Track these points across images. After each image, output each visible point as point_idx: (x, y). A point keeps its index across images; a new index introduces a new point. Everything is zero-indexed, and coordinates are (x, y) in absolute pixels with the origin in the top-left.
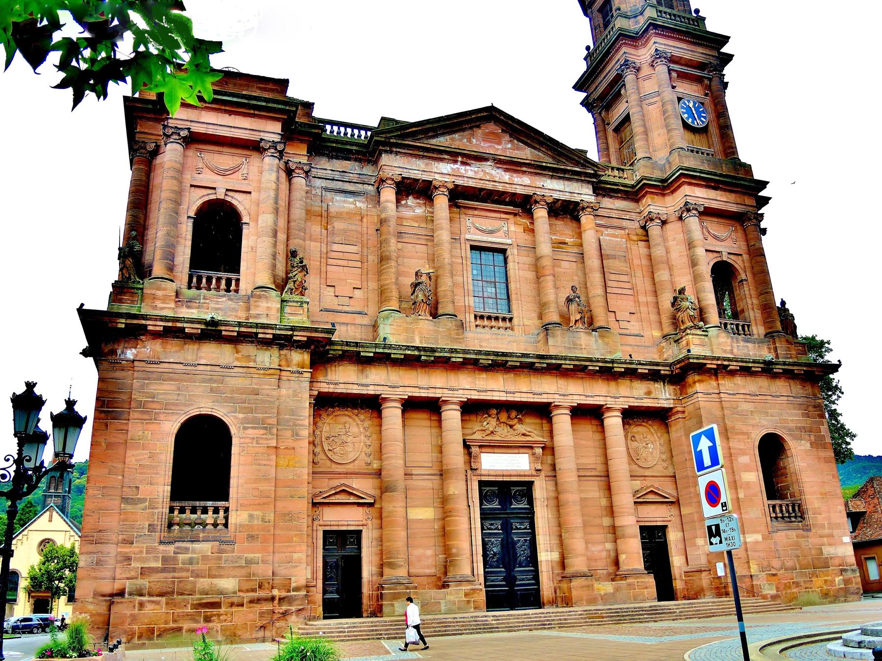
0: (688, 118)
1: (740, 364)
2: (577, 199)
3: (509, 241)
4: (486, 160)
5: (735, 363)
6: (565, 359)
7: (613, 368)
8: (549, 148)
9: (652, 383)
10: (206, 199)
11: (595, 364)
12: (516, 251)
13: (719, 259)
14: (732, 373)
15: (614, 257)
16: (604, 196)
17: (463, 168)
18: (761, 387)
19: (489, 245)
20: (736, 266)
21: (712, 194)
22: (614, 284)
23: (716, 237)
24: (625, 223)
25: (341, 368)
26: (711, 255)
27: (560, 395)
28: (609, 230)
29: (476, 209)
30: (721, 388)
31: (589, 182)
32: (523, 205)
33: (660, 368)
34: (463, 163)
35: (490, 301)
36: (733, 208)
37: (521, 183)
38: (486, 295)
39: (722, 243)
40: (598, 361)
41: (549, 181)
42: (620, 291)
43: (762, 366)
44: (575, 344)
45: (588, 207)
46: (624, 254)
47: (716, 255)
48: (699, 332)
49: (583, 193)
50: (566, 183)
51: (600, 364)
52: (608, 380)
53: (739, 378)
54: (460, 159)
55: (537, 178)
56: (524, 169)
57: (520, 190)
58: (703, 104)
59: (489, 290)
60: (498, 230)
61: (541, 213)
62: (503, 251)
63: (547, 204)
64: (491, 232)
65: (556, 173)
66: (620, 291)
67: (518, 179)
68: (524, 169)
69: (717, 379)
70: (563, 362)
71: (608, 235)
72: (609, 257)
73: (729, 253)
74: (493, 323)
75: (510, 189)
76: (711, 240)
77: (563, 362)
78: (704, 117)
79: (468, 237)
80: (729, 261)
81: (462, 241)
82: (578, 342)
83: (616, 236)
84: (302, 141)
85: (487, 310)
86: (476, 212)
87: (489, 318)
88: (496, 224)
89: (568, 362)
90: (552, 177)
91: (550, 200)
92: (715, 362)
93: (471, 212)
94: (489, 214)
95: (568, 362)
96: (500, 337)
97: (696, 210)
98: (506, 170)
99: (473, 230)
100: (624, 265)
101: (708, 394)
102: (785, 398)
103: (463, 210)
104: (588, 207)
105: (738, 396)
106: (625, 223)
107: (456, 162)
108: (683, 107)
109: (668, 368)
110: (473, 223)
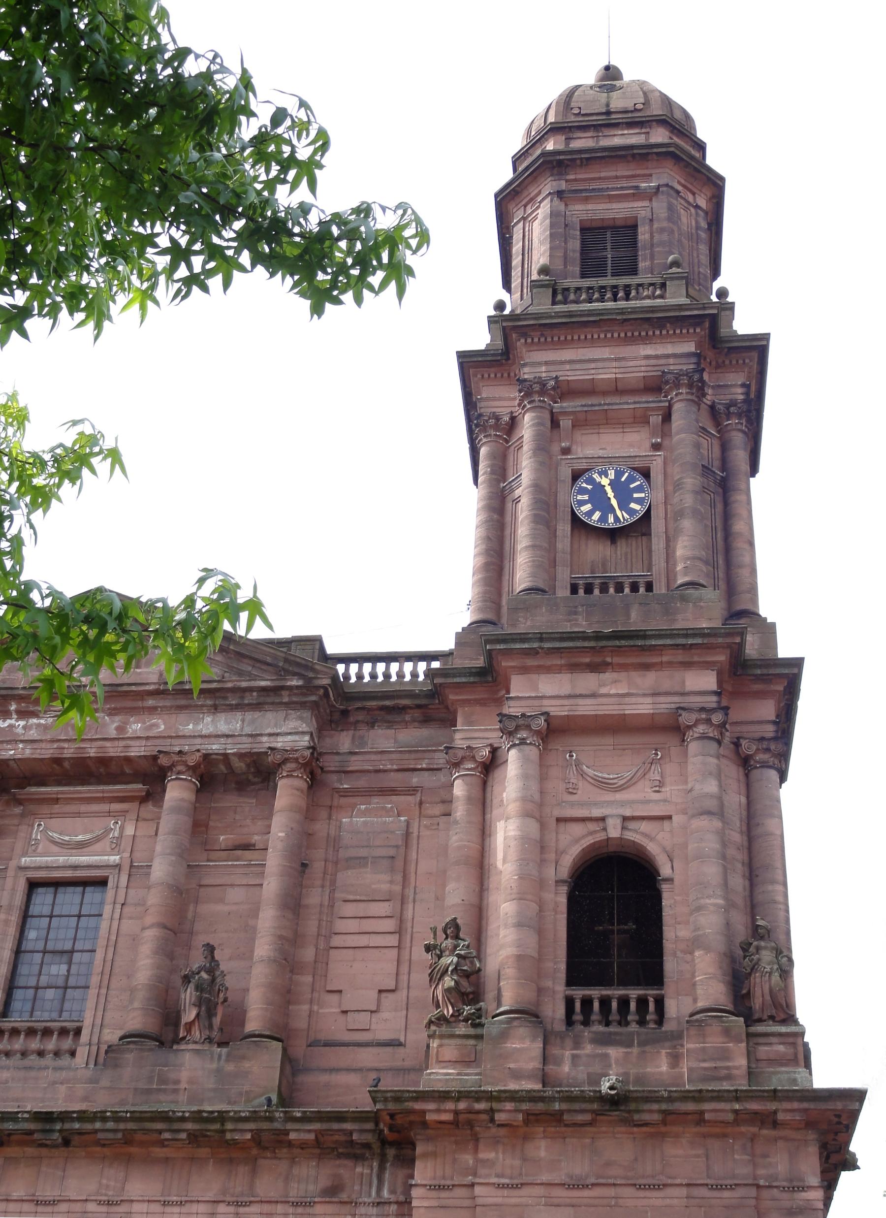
0: (590, 514)
2: (266, 742)
3: (114, 859)
5: (509, 1106)
6: (104, 1119)
7: (287, 1133)
9: (349, 1163)
11: (176, 1126)
12: (124, 879)
14: (518, 1134)
16: (372, 725)
17: (22, 723)
18: (608, 1164)
19: (69, 874)
21: (587, 682)
23: (602, 784)
24: (415, 780)
26: (577, 829)
27: (100, 1203)
28: (375, 800)
29: (56, 801)
30: (482, 1171)
31: (303, 705)
32: (148, 777)
33: (348, 1126)
34: (23, 714)
35: (50, 994)
36: (643, 707)
37: (138, 734)
38: (44, 981)
39: (619, 796)
40: (183, 1119)
41: (208, 719)
42: (363, 940)
44: (163, 1080)
46: (392, 852)
47: (592, 826)
49: (287, 732)
50: (249, 716)
51: (189, 1126)
52: (231, 1161)
54: (13, 707)
55: (183, 716)
56: (151, 702)
57: (137, 750)
58: (646, 474)
59: (54, 970)
60: (98, 839)
61: (177, 792)
62: (102, 883)
63: (190, 768)
65: (217, 698)
66: (363, 940)
67: (135, 727)
69: (476, 1150)
70: (98, 1125)
71: (364, 814)
74: (35, 1044)
75: (113, 750)
77: (98, 1125)
78: (639, 501)
79: (25, 861)
81: (11, 873)
82: (173, 1076)
83: (388, 812)
85: (37, 1014)
87: (31, 1032)
88: (98, 825)
89: (110, 1125)
91: (192, 760)
92: (450, 1105)
93: (45, 809)
94: (84, 808)
95: (110, 1125)
96: (33, 1074)
97: (528, 727)
100: (386, 877)
101: (440, 1188)
103: (32, 807)
104: (285, 761)
105: (525, 1191)
106: (415, 780)
108: (582, 491)
109: (370, 1126)
110: (44, 832)
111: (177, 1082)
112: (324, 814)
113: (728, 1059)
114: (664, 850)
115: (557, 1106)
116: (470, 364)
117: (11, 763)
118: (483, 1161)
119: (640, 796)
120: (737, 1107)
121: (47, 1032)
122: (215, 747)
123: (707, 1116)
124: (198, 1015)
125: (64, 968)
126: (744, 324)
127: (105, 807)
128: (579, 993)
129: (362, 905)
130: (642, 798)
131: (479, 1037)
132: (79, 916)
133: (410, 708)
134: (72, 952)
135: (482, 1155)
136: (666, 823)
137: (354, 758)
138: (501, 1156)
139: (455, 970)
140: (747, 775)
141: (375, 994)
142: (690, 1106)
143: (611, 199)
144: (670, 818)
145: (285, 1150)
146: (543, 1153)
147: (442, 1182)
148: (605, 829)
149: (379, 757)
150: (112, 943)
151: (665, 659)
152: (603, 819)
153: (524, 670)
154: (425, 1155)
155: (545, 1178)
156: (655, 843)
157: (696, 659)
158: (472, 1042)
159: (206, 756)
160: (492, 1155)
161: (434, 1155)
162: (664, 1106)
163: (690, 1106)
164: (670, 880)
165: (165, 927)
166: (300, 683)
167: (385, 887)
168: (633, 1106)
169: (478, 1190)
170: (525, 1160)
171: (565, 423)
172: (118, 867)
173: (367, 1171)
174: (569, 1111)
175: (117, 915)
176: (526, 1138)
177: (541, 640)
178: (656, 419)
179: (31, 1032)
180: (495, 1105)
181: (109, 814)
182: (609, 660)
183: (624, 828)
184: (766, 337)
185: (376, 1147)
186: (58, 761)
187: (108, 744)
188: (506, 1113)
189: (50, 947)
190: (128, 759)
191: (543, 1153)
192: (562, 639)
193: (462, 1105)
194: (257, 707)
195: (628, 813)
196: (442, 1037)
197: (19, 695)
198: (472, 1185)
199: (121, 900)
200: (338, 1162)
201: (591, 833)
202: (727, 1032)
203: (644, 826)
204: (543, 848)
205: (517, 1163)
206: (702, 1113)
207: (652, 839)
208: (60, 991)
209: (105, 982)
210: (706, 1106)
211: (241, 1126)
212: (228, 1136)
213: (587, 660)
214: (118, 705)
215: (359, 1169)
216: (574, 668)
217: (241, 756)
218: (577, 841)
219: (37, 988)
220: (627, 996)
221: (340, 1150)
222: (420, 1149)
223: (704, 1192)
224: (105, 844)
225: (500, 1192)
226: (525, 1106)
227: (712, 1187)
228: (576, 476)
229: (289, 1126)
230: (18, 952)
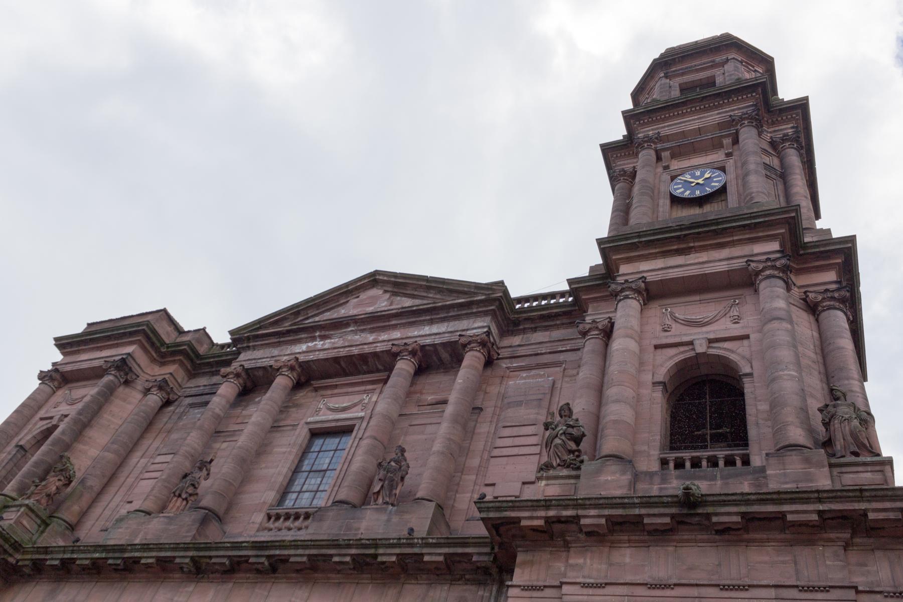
1: (607, 512)
3: (362, 414)
4: (347, 325)
5: (593, 512)
8: (440, 291)
10: (45, 427)
13: (692, 354)
15: (519, 404)
18: (690, 569)
19: (333, 424)
20: (732, 357)
22: (508, 442)
24: (562, 357)
25: (38, 587)
29: (336, 386)
42: (515, 451)
43: (673, 510)
45: (469, 343)
46: (540, 396)
48: (565, 472)
51: (353, 551)
53: (628, 551)
54: (317, 334)
59: (313, 481)
60: (355, 405)
64: (344, 409)
66: (515, 451)
67: (384, 336)
68: (393, 322)
70: (292, 552)
72: (510, 405)
73: (711, 341)
76: (676, 328)
77: (292, 552)
80: (712, 351)
83: (541, 376)
84: (174, 362)
86: (336, 391)
88: (356, 399)
90: (431, 322)
92: (542, 513)
94: (350, 390)
95: (300, 552)
98: (372, 331)
99: (324, 410)
102: (772, 593)
104: (469, 343)
107: (313, 339)
109: (487, 550)
111: (359, 529)
112: (498, 380)
113: (811, 481)
114: (743, 357)
115: (637, 511)
116: (610, 151)
117: (311, 364)
118: (572, 566)
119: (723, 327)
120: (821, 508)
121: (297, 517)
122: (428, 341)
123: (790, 517)
124: (382, 486)
125: (319, 479)
126: (787, 91)
127: (363, 388)
128: (672, 456)
129: (515, 429)
130: (724, 327)
131: (577, 477)
132: (336, 450)
133: (559, 315)
134: (325, 471)
135: (571, 561)
136: (745, 342)
137: (520, 348)
138: (588, 561)
139: (564, 433)
140: (817, 320)
141: (519, 485)
142: (770, 508)
143: (698, 71)
144: (747, 337)
145: (424, 576)
146: (627, 560)
147: (535, 583)
148: (694, 349)
149: (537, 346)
150: (348, 460)
151: (735, 238)
152: (691, 343)
153: (629, 260)
154: (524, 563)
155: (629, 578)
156: (736, 353)
157: (761, 234)
158: (572, 481)
159: (423, 347)
160: (581, 561)
161: (531, 563)
162: (743, 509)
163: (770, 508)
164: (750, 375)
165: (375, 438)
166: (483, 297)
167: (532, 416)
168: (710, 510)
169: (565, 589)
170: (611, 565)
171: (665, 155)
172: (362, 418)
173: (487, 594)
174: (649, 515)
175: (355, 445)
176: (613, 545)
177: (639, 237)
178: (727, 141)
179: (287, 517)
180: (581, 512)
181: (365, 392)
182: (692, 245)
183: (709, 347)
184: (806, 99)
185: (494, 571)
186: (336, 360)
187: (366, 346)
188: (591, 518)
189: (314, 468)
190: (375, 355)
191: (627, 560)
192: (654, 234)
193: (552, 513)
194: (457, 318)
195: (712, 336)
196: (548, 478)
197: (320, 325)
198: (560, 587)
199: (360, 435)
200: (465, 587)
201: (682, 353)
202: (807, 461)
203: (726, 345)
204: (641, 363)
205: (604, 567)
206: (782, 516)
207: (732, 351)
208: (313, 494)
209: (338, 484)
210: (786, 508)
211: (389, 551)
212: (380, 559)
213: (675, 247)
214: (375, 325)
215: (480, 593)
216: (665, 254)
217: (444, 345)
218: (671, 358)
219: (299, 492)
220: (715, 456)
221: (467, 577)
222: (520, 558)
223: (794, 593)
224: (359, 407)
225: (585, 591)
226: (607, 512)
227: (803, 589)
228: (673, 178)
229: (425, 551)
230: (296, 471)
